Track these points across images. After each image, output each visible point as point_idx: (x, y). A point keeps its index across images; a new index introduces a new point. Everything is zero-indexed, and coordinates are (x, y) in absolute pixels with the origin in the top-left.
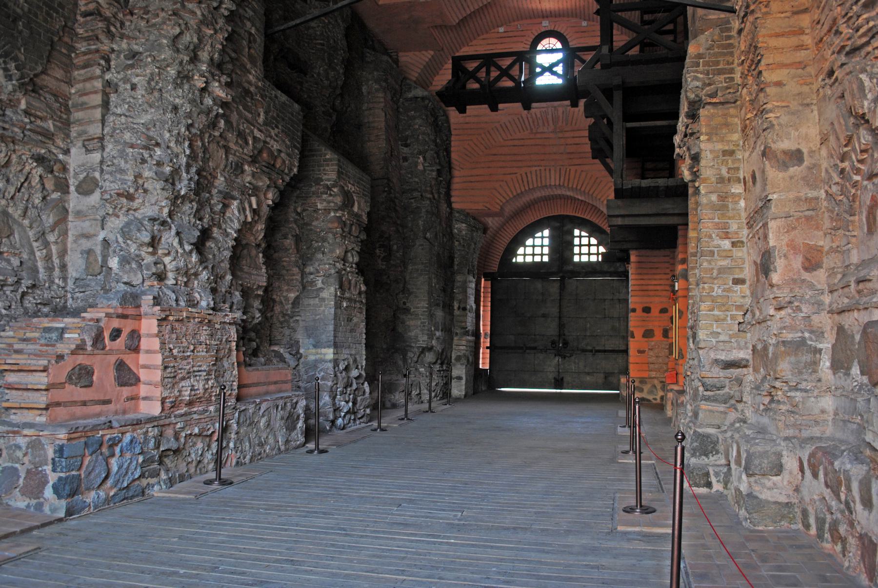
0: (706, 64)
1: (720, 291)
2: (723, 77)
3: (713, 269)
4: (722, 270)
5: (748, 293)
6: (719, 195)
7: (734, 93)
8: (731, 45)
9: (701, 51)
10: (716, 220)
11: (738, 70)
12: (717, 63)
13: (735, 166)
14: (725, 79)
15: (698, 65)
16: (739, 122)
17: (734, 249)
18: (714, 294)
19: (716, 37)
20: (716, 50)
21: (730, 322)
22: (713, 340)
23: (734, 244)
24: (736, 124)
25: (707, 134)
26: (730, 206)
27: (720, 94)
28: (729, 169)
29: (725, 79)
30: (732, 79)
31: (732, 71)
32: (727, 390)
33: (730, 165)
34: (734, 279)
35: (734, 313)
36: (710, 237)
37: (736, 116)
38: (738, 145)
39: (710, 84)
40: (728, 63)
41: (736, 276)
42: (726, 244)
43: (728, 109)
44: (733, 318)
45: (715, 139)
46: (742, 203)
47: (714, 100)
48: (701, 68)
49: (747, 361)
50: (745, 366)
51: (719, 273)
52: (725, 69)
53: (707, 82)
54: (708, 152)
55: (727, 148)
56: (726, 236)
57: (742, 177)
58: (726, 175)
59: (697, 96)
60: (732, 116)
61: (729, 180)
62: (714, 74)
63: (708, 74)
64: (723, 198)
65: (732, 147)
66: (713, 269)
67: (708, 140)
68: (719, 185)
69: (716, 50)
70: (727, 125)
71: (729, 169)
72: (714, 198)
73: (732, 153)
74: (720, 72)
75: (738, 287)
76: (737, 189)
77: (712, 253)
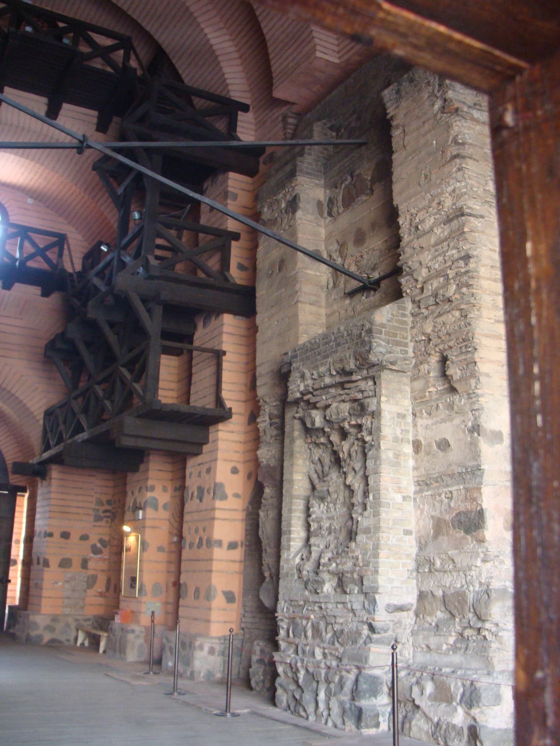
0: (387, 333)
1: (394, 540)
2: (399, 349)
3: (389, 519)
4: (396, 522)
5: (414, 543)
6: (394, 453)
7: (409, 364)
8: (405, 323)
9: (384, 321)
10: (392, 475)
11: (411, 345)
12: (395, 335)
13: (407, 428)
14: (401, 350)
15: (381, 333)
16: (409, 390)
17: (404, 503)
18: (390, 542)
19: (395, 313)
20: (395, 324)
21: (401, 569)
22: (389, 586)
23: (404, 498)
24: (407, 392)
25: (386, 396)
26: (402, 464)
27: (399, 363)
28: (402, 430)
29: (401, 350)
30: (406, 352)
31: (406, 345)
32: (390, 633)
33: (403, 427)
34: (404, 530)
35: (404, 561)
36: (387, 490)
37: (408, 385)
38: (408, 411)
39: (390, 353)
40: (403, 338)
41: (406, 528)
42: (398, 498)
43: (402, 377)
44: (404, 565)
45: (391, 402)
46: (411, 463)
47: (394, 368)
48: (383, 336)
49: (412, 605)
50: (408, 610)
51: (394, 524)
52: (401, 342)
53: (389, 350)
54: (386, 412)
55: (400, 411)
56: (399, 490)
57: (411, 440)
58: (400, 436)
59: (378, 360)
60: (405, 384)
61: (402, 440)
62: (393, 345)
63: (388, 343)
64: (397, 455)
65: (405, 412)
66: (389, 519)
67: (387, 401)
68: (395, 444)
69: (395, 324)
70: (401, 391)
71: (402, 430)
72: (390, 454)
73: (403, 416)
74: (398, 344)
75: (407, 538)
76: (408, 449)
77: (388, 504)
